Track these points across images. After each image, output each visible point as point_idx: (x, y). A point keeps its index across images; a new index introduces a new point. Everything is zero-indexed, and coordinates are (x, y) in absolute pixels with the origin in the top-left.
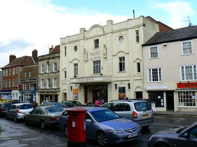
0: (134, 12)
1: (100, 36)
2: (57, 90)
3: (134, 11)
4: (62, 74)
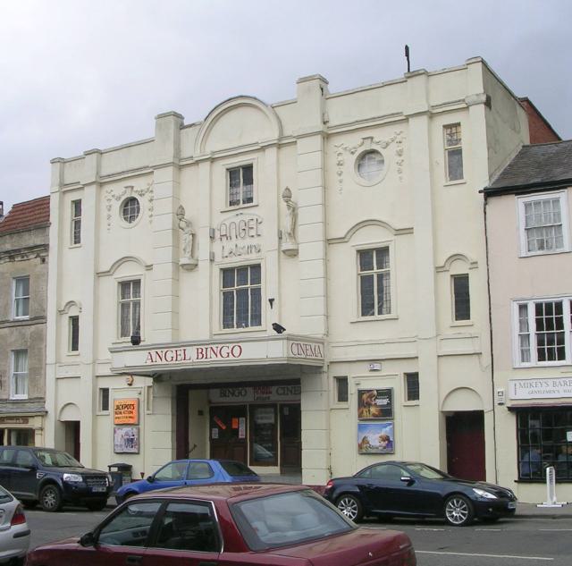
0: (407, 55)
1: (263, 149)
2: (33, 407)
3: (407, 48)
4: (55, 332)
